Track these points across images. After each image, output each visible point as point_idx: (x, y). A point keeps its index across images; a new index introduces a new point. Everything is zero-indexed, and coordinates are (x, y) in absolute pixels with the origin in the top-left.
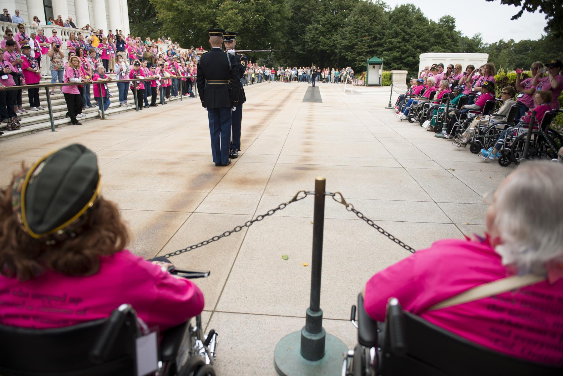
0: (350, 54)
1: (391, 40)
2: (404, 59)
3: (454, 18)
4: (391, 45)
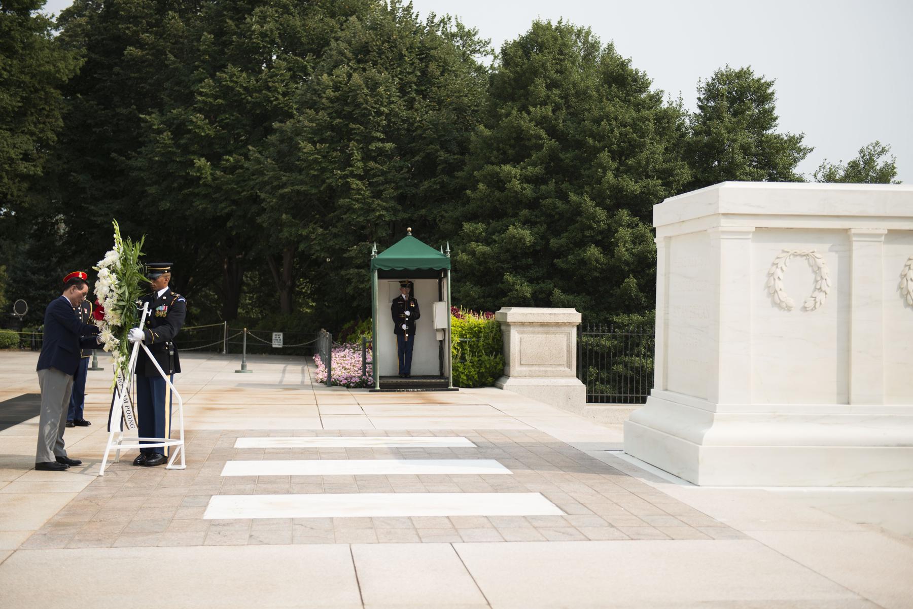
0: (320, 230)
1: (497, 169)
2: (560, 253)
3: (767, 79)
4: (497, 194)
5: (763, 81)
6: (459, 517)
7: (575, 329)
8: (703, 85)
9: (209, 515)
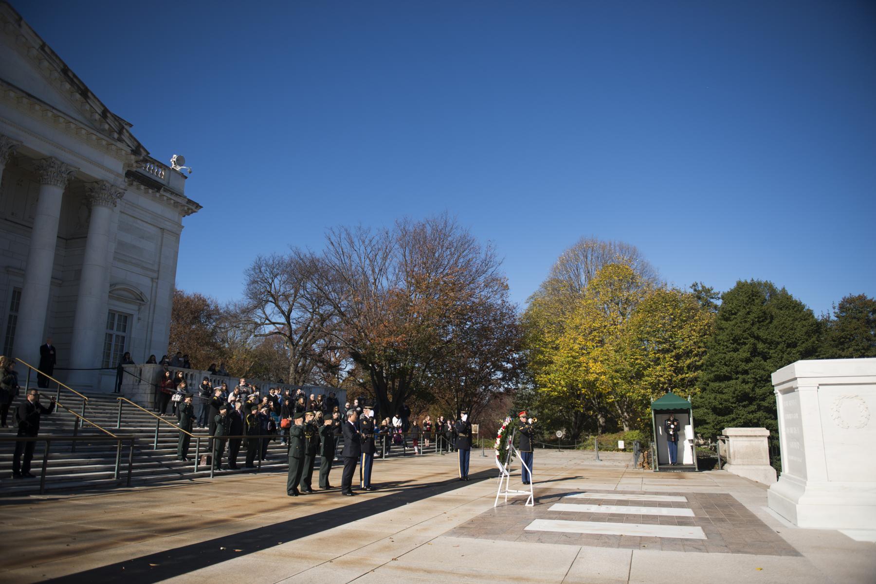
1: (723, 356)
5: (873, 300)
6: (647, 537)
7: (767, 439)
8: (837, 305)
9: (527, 528)
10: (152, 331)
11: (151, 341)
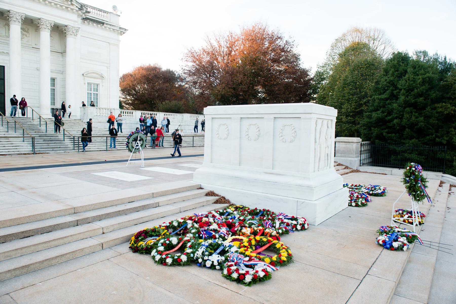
10: (110, 91)
11: (110, 95)
